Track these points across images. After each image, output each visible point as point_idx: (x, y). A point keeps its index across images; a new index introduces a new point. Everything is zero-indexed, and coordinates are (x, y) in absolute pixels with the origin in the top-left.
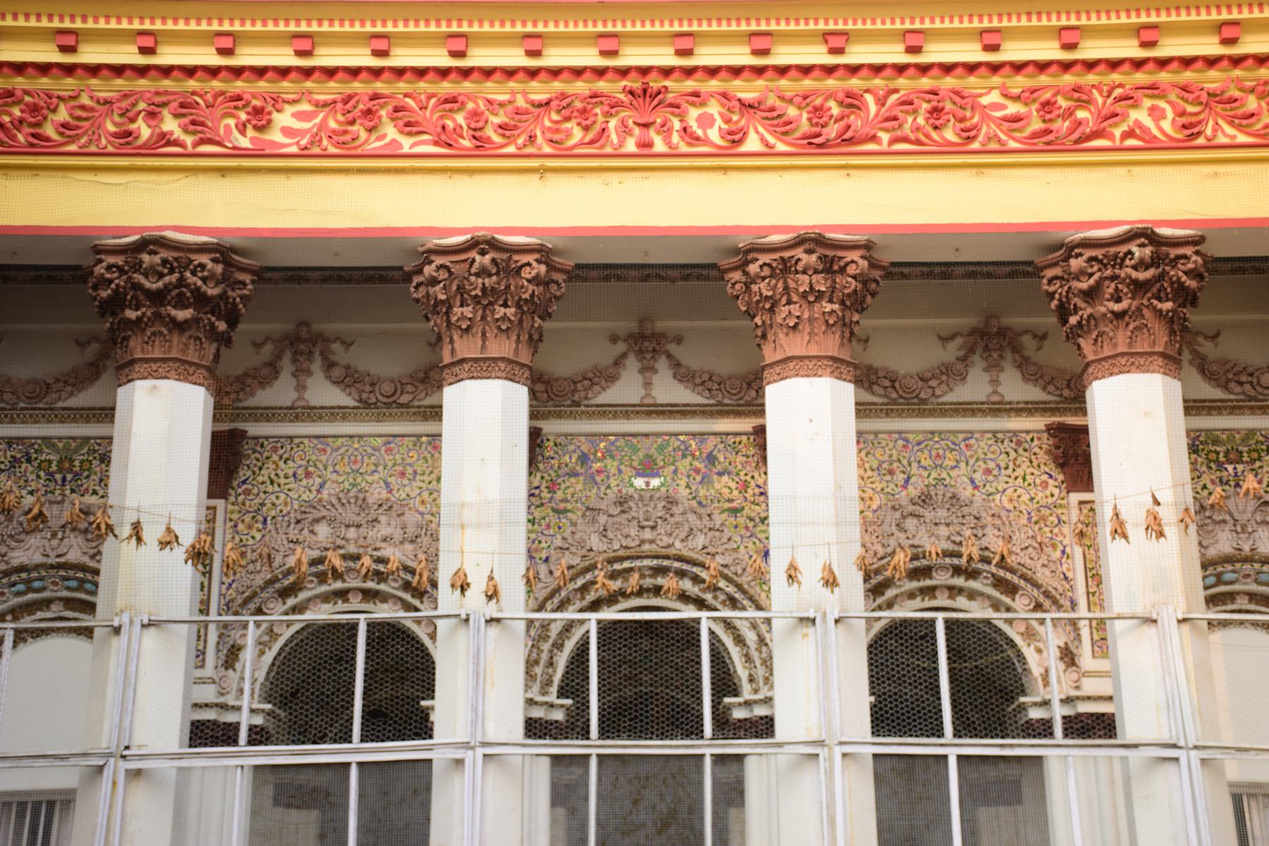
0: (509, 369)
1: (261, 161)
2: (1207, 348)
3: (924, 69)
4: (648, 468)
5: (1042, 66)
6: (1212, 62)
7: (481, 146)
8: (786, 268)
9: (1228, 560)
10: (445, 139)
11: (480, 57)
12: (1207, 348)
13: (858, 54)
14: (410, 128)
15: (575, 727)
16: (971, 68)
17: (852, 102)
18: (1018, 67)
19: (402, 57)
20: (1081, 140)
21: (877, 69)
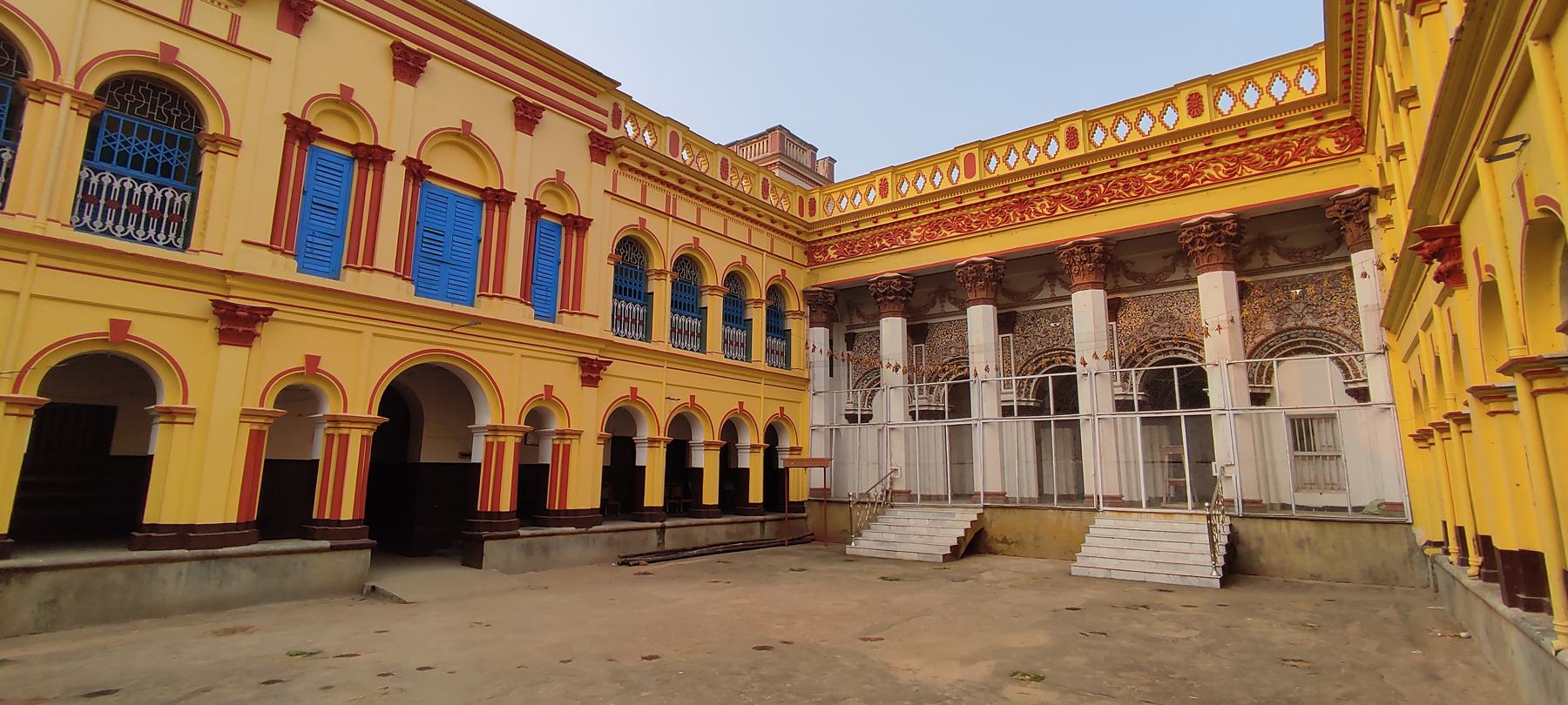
0: (985, 301)
1: (909, 247)
2: (1281, 243)
3: (1120, 172)
4: (1055, 319)
5: (1167, 161)
6: (1237, 145)
7: (971, 230)
8: (1073, 253)
9: (1290, 329)
10: (959, 230)
11: (967, 202)
12: (1281, 243)
13: (1093, 172)
14: (949, 228)
15: (1042, 409)
16: (1138, 167)
17: (1094, 189)
18: (1157, 163)
19: (944, 208)
20: (1185, 184)
21: (1102, 176)
